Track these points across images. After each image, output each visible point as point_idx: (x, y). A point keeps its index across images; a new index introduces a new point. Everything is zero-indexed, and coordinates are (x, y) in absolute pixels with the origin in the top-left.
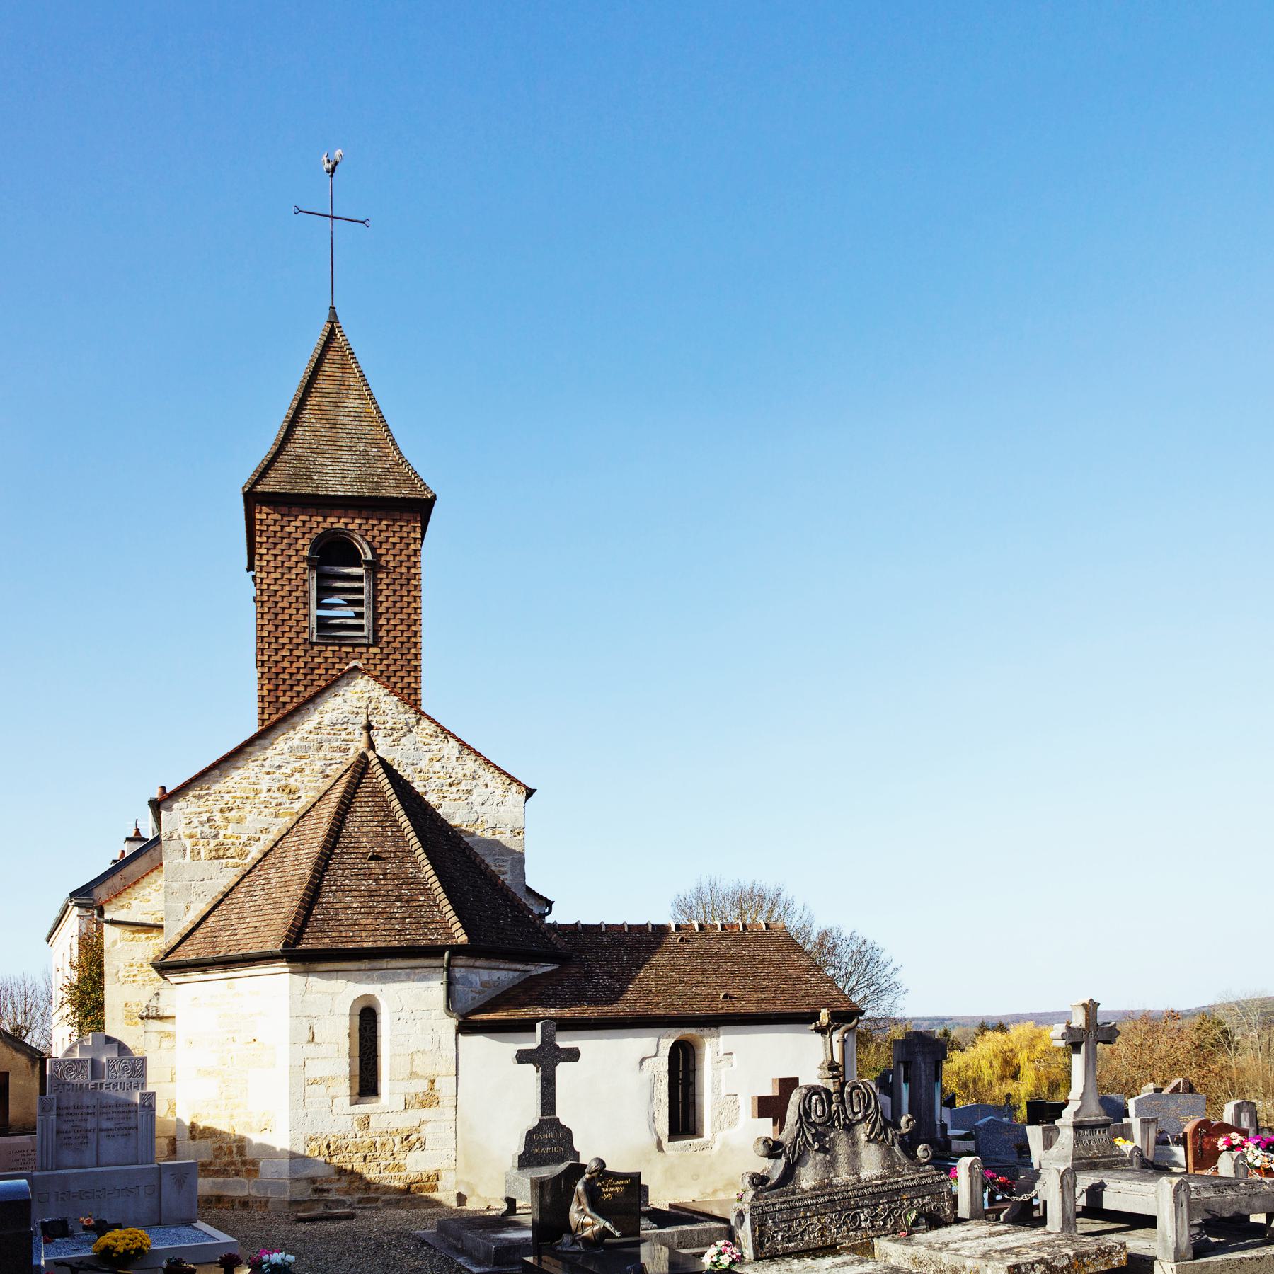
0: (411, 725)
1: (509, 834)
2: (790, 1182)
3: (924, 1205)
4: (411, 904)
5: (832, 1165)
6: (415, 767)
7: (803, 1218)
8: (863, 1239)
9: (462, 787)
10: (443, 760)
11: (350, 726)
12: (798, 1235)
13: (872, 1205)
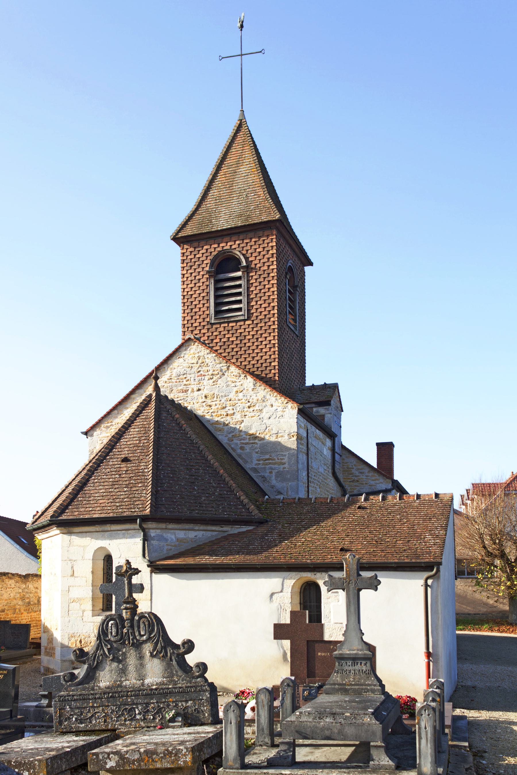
0: (224, 371)
1: (286, 437)
2: (91, 681)
3: (187, 708)
4: (132, 489)
5: (123, 671)
6: (227, 397)
7: (92, 707)
8: (137, 728)
9: (257, 408)
10: (244, 392)
11: (188, 375)
12: (87, 719)
13: (145, 703)
